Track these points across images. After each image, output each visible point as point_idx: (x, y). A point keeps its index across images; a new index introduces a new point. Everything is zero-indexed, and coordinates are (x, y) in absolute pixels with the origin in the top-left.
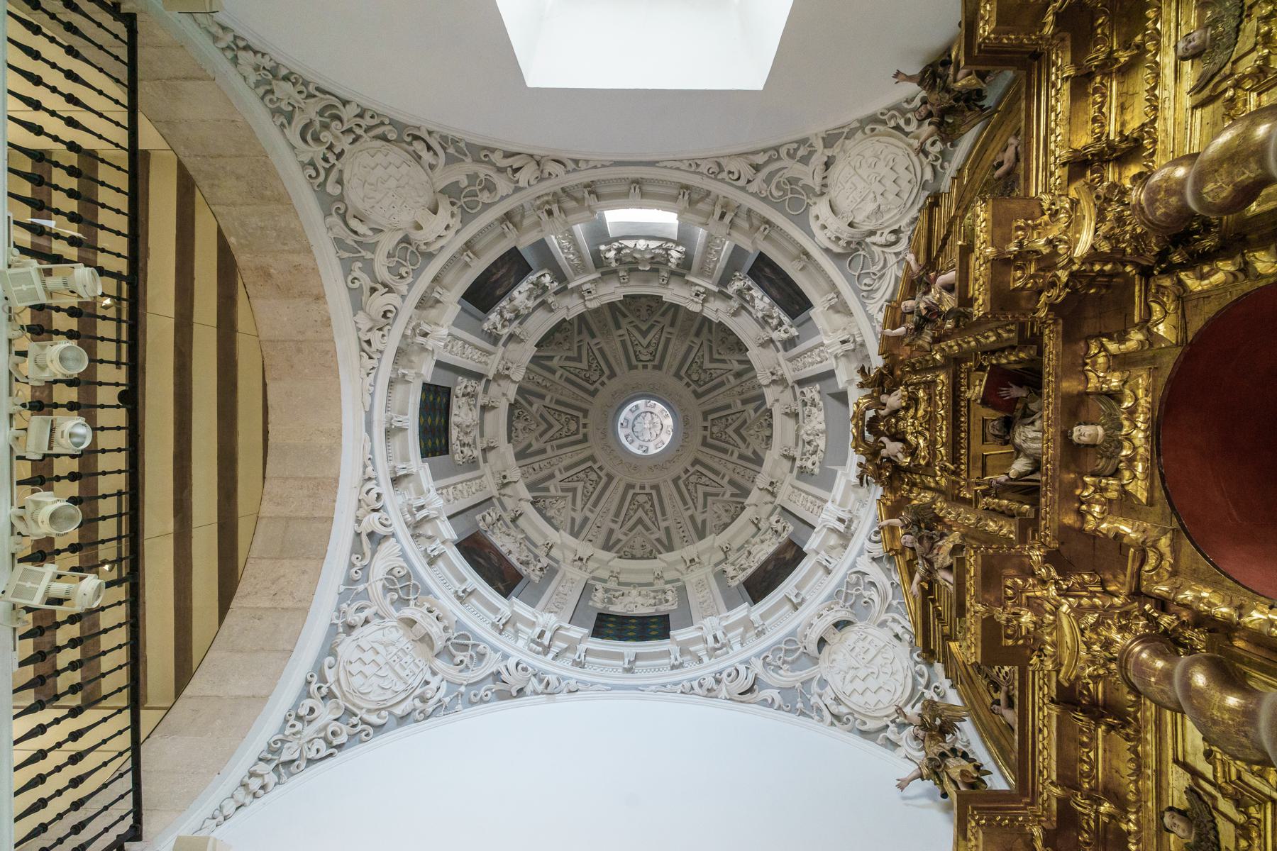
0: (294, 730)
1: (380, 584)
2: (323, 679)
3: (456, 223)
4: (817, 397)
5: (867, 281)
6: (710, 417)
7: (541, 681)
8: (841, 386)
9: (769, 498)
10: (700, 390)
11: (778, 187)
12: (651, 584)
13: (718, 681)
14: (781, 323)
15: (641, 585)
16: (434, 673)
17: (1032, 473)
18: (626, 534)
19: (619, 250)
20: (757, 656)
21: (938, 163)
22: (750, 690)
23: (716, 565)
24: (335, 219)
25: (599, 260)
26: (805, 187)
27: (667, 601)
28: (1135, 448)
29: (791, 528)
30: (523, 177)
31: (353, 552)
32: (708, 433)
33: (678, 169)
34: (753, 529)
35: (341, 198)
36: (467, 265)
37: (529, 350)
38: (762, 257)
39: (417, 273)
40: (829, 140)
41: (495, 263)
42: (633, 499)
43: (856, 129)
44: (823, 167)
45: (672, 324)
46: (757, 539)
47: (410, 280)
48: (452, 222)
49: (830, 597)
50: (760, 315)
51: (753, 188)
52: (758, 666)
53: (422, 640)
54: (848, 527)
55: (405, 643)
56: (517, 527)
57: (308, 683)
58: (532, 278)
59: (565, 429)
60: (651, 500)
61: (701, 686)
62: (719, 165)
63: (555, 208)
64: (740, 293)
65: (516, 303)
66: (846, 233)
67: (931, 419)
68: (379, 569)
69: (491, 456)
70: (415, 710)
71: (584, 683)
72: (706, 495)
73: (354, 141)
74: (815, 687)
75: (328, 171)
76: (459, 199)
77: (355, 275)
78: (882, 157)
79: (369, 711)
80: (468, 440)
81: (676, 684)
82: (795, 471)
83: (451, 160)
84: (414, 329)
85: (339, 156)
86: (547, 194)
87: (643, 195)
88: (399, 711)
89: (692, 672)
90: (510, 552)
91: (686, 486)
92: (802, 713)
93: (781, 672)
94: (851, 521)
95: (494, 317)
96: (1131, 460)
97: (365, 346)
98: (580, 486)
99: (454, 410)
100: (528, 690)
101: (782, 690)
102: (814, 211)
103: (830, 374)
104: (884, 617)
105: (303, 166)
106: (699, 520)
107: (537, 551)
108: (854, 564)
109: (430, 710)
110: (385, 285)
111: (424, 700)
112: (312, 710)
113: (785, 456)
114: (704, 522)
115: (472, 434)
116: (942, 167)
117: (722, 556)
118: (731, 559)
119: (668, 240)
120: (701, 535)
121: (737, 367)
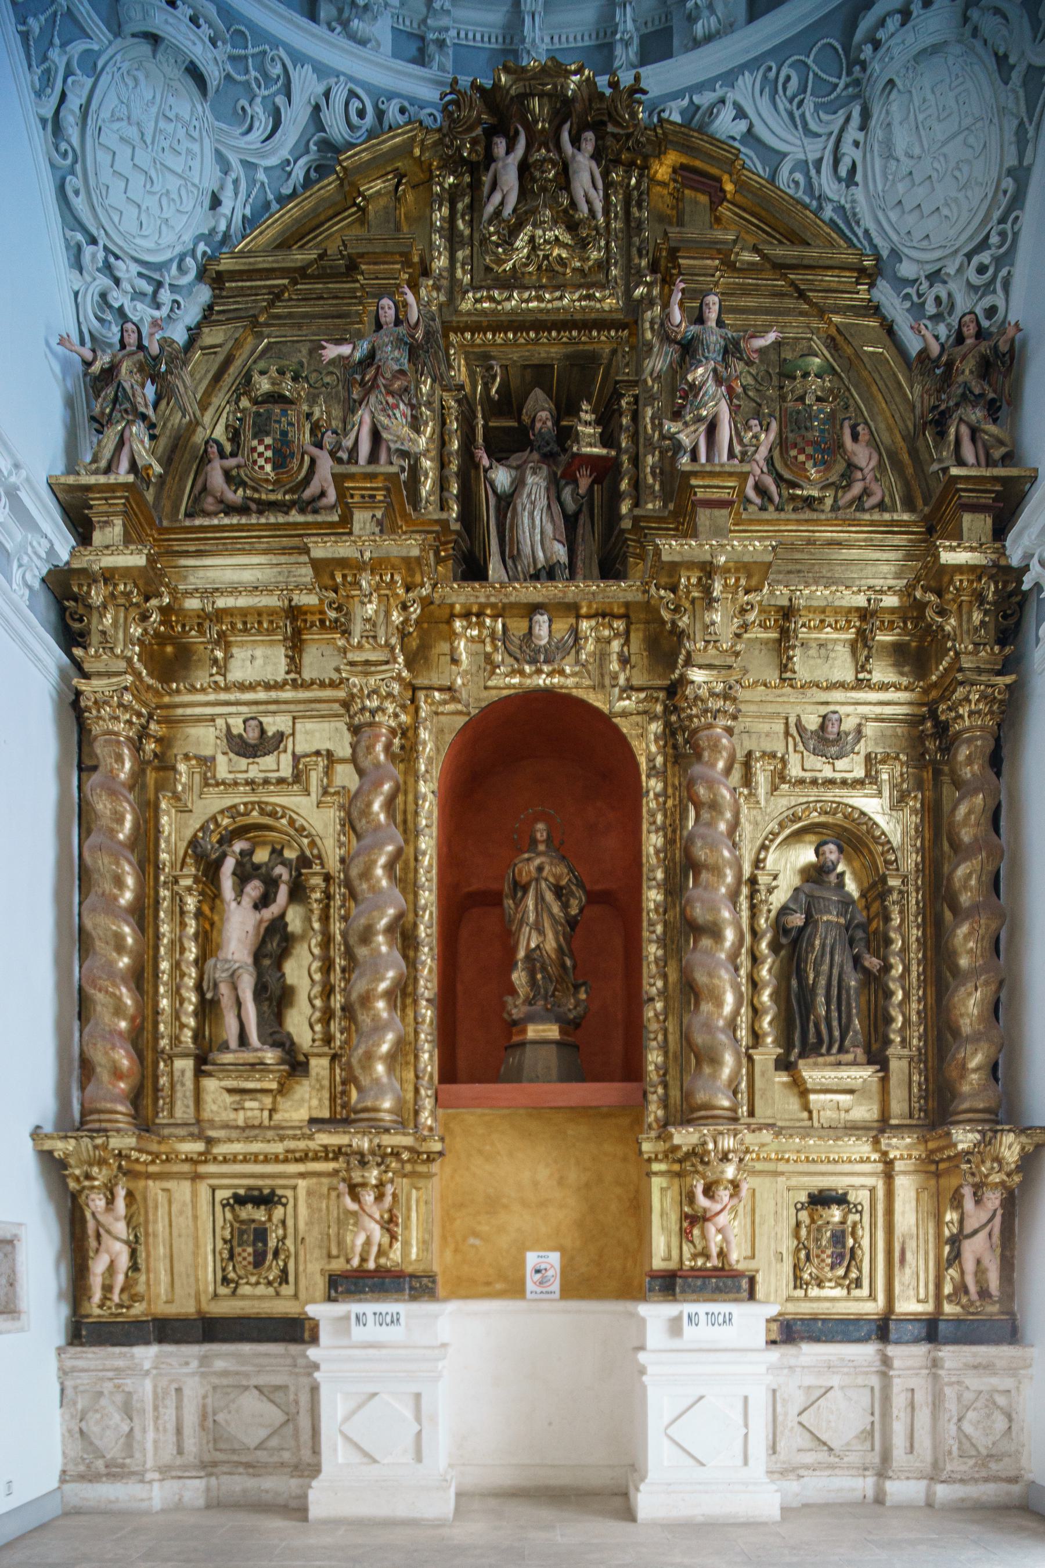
5: (794, 85)
17: (495, 492)
28: (530, 676)
96: (522, 673)
104: (234, 159)
116: (907, 296)
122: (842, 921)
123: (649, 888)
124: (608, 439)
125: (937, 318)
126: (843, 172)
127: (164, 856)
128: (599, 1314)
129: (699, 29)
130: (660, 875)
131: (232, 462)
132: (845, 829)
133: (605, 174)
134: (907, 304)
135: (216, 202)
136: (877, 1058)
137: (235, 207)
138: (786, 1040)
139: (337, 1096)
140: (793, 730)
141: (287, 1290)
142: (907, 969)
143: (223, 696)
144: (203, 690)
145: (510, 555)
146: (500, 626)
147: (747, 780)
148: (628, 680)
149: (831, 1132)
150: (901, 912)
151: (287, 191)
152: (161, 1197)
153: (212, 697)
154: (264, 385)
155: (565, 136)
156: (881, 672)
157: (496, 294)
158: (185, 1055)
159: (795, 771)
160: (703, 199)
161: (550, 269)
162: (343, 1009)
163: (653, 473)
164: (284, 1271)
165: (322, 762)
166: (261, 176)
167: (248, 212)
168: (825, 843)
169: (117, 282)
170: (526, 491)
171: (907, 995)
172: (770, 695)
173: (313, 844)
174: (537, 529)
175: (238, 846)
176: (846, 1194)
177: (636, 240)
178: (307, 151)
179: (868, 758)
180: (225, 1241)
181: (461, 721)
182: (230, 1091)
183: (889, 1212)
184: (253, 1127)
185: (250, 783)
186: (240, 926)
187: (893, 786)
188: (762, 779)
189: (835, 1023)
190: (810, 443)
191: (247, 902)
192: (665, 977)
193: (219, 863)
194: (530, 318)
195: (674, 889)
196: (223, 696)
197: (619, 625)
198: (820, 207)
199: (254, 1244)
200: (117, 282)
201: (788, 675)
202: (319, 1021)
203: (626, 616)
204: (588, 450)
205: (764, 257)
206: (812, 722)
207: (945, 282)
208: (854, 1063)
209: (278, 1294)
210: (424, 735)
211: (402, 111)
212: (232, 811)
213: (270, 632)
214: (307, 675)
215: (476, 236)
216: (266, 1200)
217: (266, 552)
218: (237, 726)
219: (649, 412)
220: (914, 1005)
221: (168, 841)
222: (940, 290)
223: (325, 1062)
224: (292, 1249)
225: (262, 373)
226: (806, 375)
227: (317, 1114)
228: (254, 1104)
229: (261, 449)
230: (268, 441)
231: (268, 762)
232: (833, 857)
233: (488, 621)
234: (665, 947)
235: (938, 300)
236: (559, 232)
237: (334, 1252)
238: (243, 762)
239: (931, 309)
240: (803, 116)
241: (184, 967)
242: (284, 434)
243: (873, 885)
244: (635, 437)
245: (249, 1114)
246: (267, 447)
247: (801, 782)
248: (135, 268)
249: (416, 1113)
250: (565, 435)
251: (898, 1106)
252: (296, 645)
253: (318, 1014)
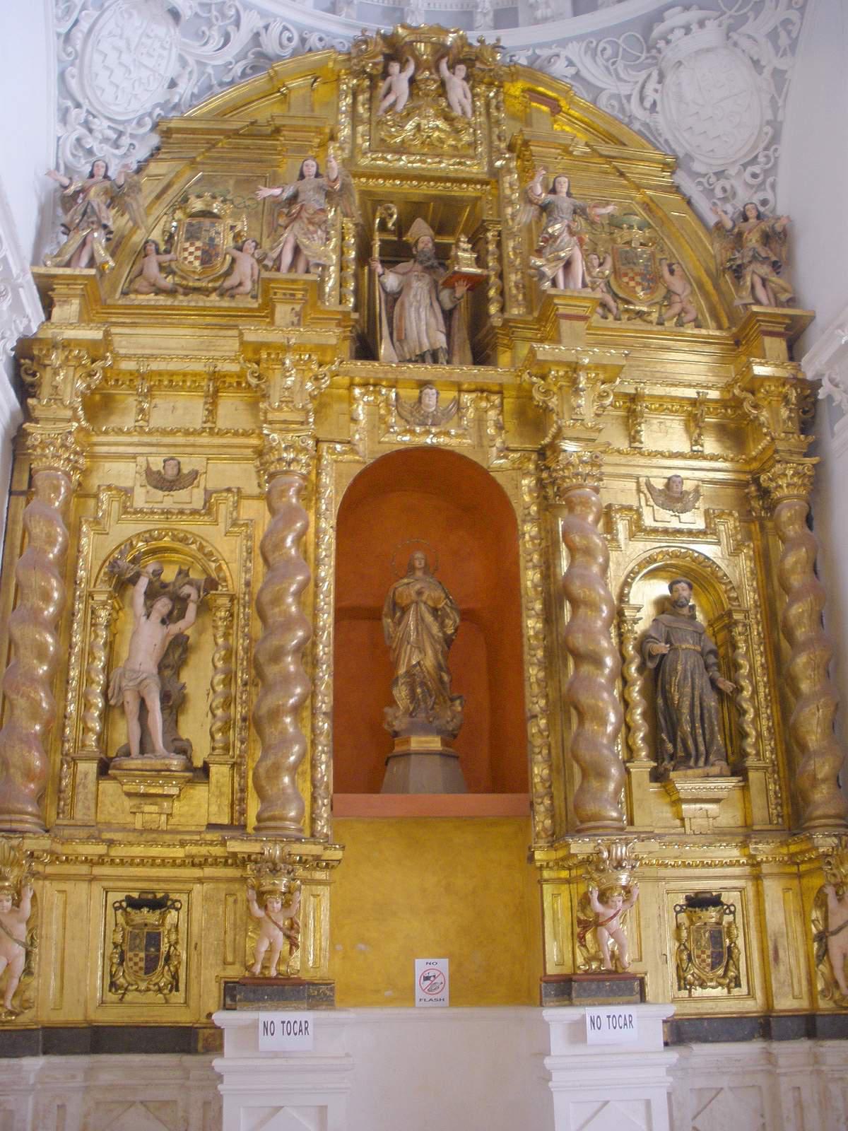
26: (743, 20)
40: (779, 75)
43: (775, 113)
66: (670, 54)
67: (433, 148)
96: (412, 432)
116: (700, 183)
122: (698, 648)
123: (529, 617)
124: (480, 262)
125: (725, 200)
126: (648, 104)
127: (81, 573)
128: (491, 1024)
129: (539, 14)
130: (538, 606)
131: (168, 257)
132: (693, 570)
133: (472, 88)
134: (701, 188)
135: (173, 84)
136: (738, 770)
137: (185, 88)
138: (656, 752)
139: (238, 803)
140: (644, 488)
141: (178, 997)
142: (755, 692)
143: (146, 439)
144: (129, 433)
145: (398, 338)
146: (393, 395)
147: (610, 527)
148: (503, 442)
149: (702, 839)
150: (746, 641)
151: (227, 79)
152: (57, 899)
153: (135, 439)
154: (197, 205)
155: (444, 65)
156: (710, 445)
157: (389, 157)
158: (88, 759)
159: (648, 521)
160: (545, 108)
161: (431, 144)
162: (244, 719)
163: (517, 287)
164: (175, 977)
165: (232, 498)
166: (210, 70)
167: (196, 91)
168: (679, 582)
169: (91, 131)
170: (412, 293)
171: (757, 714)
172: (623, 460)
173: (219, 568)
174: (422, 321)
175: (151, 565)
176: (719, 896)
177: (496, 131)
179: (706, 512)
180: (116, 945)
181: (358, 469)
182: (129, 795)
183: (760, 912)
184: (151, 831)
185: (167, 512)
186: (145, 639)
187: (728, 537)
188: (622, 527)
189: (700, 739)
190: (637, 274)
191: (156, 616)
192: (546, 696)
193: (134, 581)
194: (416, 173)
195: (550, 616)
196: (146, 439)
197: (496, 399)
198: (631, 122)
199: (147, 950)
200: (91, 131)
201: (637, 444)
202: (220, 730)
203: (500, 392)
204: (465, 269)
205: (594, 150)
206: (659, 484)
207: (727, 179)
208: (721, 775)
209: (167, 1001)
210: (325, 479)
211: (321, 39)
212: (148, 537)
213: (190, 390)
214: (221, 424)
215: (374, 119)
216: (159, 904)
217: (193, 326)
218: (157, 464)
219: (511, 244)
220: (764, 722)
221: (85, 560)
222: (722, 182)
223: (225, 769)
224: (184, 956)
225: (199, 197)
226: (631, 227)
227: (214, 820)
228: (154, 808)
229: (192, 249)
230: (198, 244)
231: (182, 495)
232: (686, 593)
233: (384, 391)
234: (546, 668)
235: (724, 190)
236: (440, 123)
237: (230, 959)
238: (160, 493)
239: (719, 193)
240: (616, 70)
241: (93, 675)
242: (212, 239)
243: (720, 618)
244: (500, 259)
245: (147, 817)
246: (197, 249)
247: (655, 531)
248: (106, 123)
249: (313, 821)
250: (443, 254)
251: (759, 814)
252: (213, 400)
253: (219, 724)
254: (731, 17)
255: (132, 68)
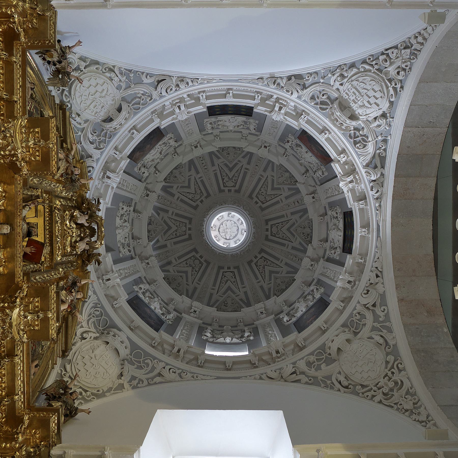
0: (405, 64)
1: (370, 139)
2: (395, 89)
3: (329, 344)
4: (121, 249)
5: (98, 313)
6: (187, 236)
7: (279, 84)
8: (110, 254)
9: (149, 186)
10: (193, 253)
11: (148, 365)
12: (221, 132)
13: (178, 85)
14: (144, 293)
15: (228, 131)
16: (338, 89)
18: (239, 161)
19: (242, 337)
20: (155, 100)
21: (64, 372)
22: (159, 82)
23: (181, 145)
24: (391, 343)
25: (255, 331)
27: (211, 124)
29: (136, 169)
30: (290, 369)
31: (385, 158)
32: (188, 226)
33: (204, 375)
34: (159, 167)
35: (388, 354)
36: (326, 322)
37: (299, 277)
38: (157, 330)
39: (351, 315)
40: (121, 387)
41: (312, 323)
42: (236, 183)
44: (124, 374)
45: (211, 295)
46: (156, 162)
47: (355, 312)
48: (330, 344)
49: (115, 135)
50: (156, 299)
51: (162, 365)
52: (155, 94)
53: (345, 108)
54: (105, 173)
55: (354, 106)
56: (305, 166)
57: (402, 87)
58: (294, 319)
59: (279, 228)
60: (224, 183)
61: (187, 83)
62: (181, 377)
63: (274, 355)
64: (169, 313)
65: (305, 305)
66: (109, 338)
68: (370, 148)
69: (322, 211)
70: (346, 70)
71: (254, 83)
72: (189, 187)
73: (377, 384)
74: (124, 85)
75: (392, 367)
76: (326, 357)
77: (383, 314)
78: (93, 377)
79: (370, 71)
80: (335, 221)
81: (201, 83)
82: (133, 204)
83: (329, 377)
84: (355, 284)
85: (386, 375)
86: (278, 362)
87: (224, 363)
88: (355, 70)
89: (194, 89)
90: (307, 152)
91: (201, 192)
92: (130, 71)
93: (142, 92)
94: (103, 177)
95: (318, 296)
97: (379, 274)
98: (270, 192)
99: (341, 239)
100: (284, 81)
101: (141, 82)
102: (128, 351)
103: (116, 262)
104: (85, 125)
105: (404, 369)
106: (193, 171)
107: (292, 152)
108: (102, 153)
109: (338, 70)
110: (368, 308)
111: (342, 76)
112: (398, 73)
113: (140, 213)
114: (190, 170)
115: (332, 224)
117: (178, 150)
118: (172, 149)
119: (212, 342)
120: (191, 162)
121: (170, 268)
178: (82, 151)
240: (91, 318)
254: (131, 359)
255: (93, 97)
